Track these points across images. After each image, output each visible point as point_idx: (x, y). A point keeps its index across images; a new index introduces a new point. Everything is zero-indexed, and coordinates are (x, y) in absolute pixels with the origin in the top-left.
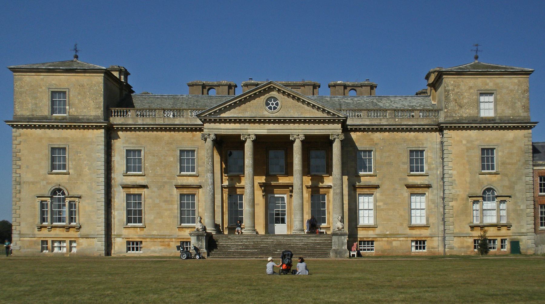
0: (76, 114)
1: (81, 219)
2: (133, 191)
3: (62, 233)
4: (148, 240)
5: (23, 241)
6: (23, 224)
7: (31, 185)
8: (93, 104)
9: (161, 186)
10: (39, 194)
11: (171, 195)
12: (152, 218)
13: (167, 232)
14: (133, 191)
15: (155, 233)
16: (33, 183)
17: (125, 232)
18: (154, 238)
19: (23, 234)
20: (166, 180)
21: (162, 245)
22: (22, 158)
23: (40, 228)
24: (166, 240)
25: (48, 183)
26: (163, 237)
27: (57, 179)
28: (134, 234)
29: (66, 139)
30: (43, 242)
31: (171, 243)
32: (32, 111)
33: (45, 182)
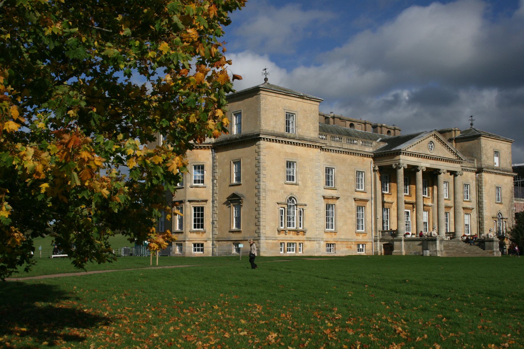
0: (302, 134)
1: (306, 225)
2: (331, 202)
3: (294, 236)
4: (339, 243)
5: (267, 243)
6: (267, 228)
7: (273, 193)
8: (312, 127)
9: (346, 200)
10: (279, 201)
11: (352, 206)
12: (341, 225)
13: (349, 237)
14: (331, 202)
15: (343, 237)
16: (275, 191)
17: (325, 236)
18: (343, 241)
19: (268, 237)
20: (349, 194)
21: (347, 247)
22: (267, 168)
23: (279, 231)
24: (350, 243)
25: (284, 192)
26: (347, 241)
27: (292, 190)
28: (331, 239)
29: (296, 154)
30: (281, 244)
31: (352, 246)
32: (274, 127)
33: (282, 191)
